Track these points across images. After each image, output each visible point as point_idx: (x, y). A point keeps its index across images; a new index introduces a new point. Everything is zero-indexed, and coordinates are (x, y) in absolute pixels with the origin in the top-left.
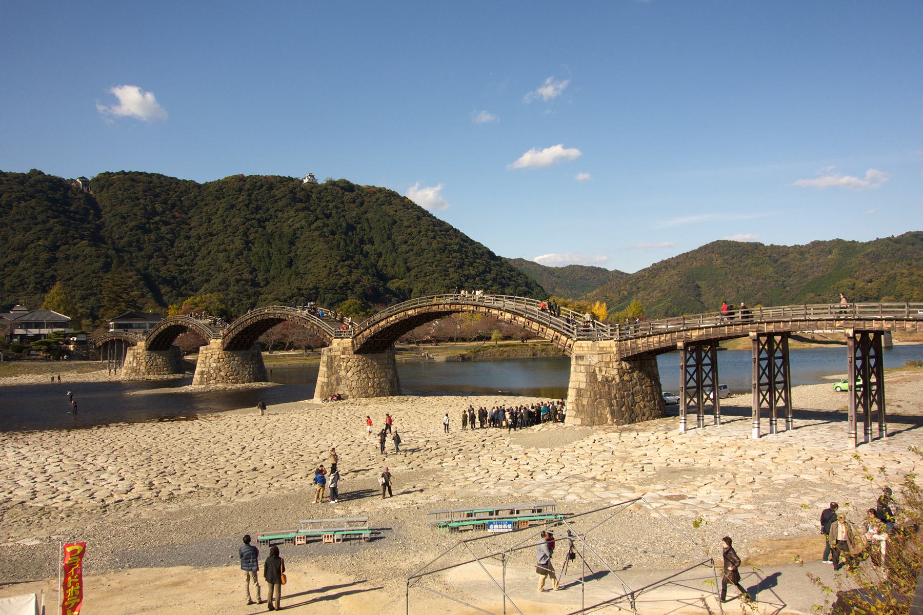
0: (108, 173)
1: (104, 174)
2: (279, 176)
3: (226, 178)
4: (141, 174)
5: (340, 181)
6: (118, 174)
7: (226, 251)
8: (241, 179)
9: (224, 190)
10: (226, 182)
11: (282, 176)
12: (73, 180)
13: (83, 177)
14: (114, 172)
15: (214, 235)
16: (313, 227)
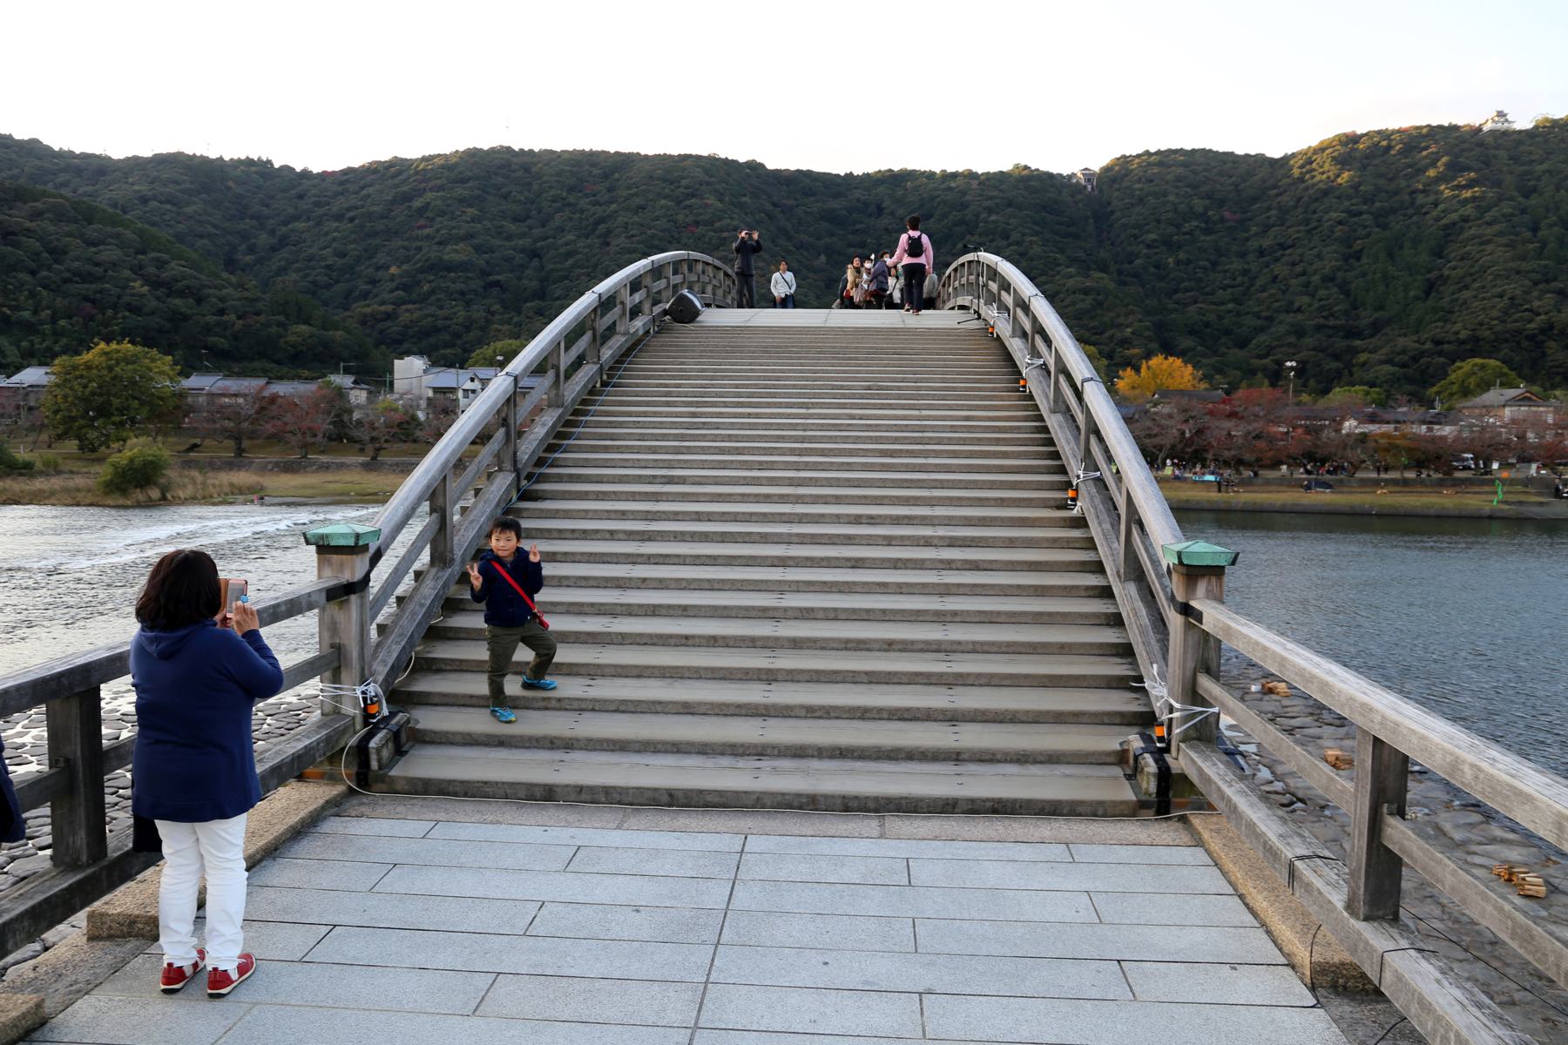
0: (1124, 157)
1: (1118, 159)
2: (1428, 126)
3: (1322, 142)
4: (1176, 151)
6: (1138, 156)
7: (1304, 273)
8: (1351, 140)
9: (1314, 165)
10: (1321, 149)
11: (1434, 124)
12: (1074, 175)
13: (1086, 169)
14: (1134, 154)
15: (1289, 247)
16: (1488, 217)
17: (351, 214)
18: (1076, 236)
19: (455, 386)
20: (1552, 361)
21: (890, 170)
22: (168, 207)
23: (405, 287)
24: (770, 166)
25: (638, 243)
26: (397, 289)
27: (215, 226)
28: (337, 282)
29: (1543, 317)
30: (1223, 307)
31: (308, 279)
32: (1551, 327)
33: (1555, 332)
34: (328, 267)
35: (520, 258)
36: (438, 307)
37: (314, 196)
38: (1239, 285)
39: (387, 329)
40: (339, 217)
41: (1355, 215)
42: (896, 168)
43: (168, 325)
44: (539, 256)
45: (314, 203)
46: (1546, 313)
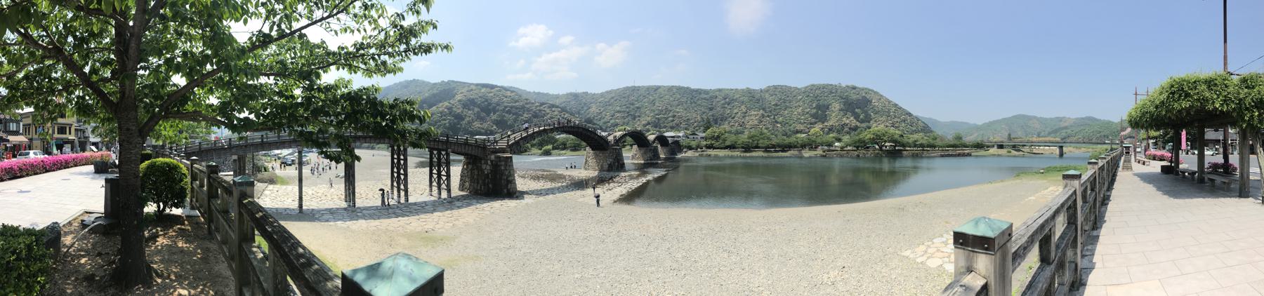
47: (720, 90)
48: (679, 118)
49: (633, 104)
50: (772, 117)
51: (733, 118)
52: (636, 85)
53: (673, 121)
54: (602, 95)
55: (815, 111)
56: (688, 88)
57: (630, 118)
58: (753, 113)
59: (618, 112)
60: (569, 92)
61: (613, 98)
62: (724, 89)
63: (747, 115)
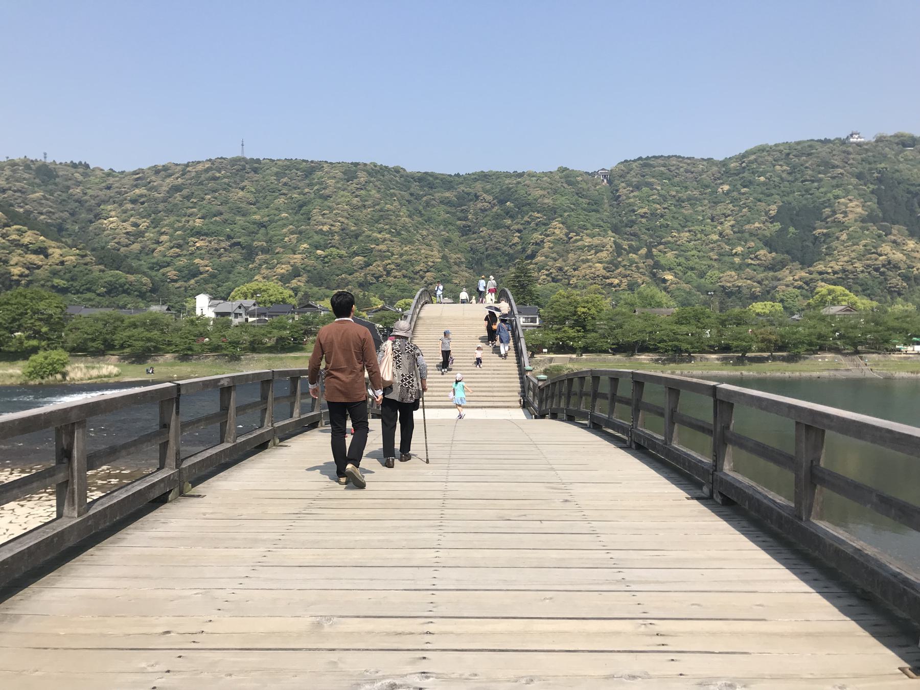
5: (896, 136)
17: (142, 200)
18: (597, 211)
19: (230, 311)
20: (890, 284)
21: (482, 172)
22: (19, 194)
23: (179, 246)
24: (409, 170)
25: (328, 218)
26: (172, 248)
27: (51, 207)
28: (133, 243)
29: (884, 257)
30: (689, 253)
31: (115, 240)
32: (889, 262)
33: (892, 266)
34: (127, 233)
35: (253, 228)
36: (200, 258)
37: (117, 187)
38: (698, 240)
39: (167, 272)
40: (134, 201)
41: (768, 196)
42: (486, 170)
43: (27, 272)
44: (264, 226)
45: (116, 192)
46: (886, 255)
47: (484, 177)
48: (383, 258)
49: (240, 212)
50: (644, 251)
51: (533, 256)
52: (248, 156)
53: (368, 264)
54: (139, 177)
55: (778, 226)
56: (397, 170)
57: (236, 255)
58: (587, 241)
59: (198, 233)
60: (17, 156)
61: (177, 189)
62: (498, 175)
63: (571, 246)
